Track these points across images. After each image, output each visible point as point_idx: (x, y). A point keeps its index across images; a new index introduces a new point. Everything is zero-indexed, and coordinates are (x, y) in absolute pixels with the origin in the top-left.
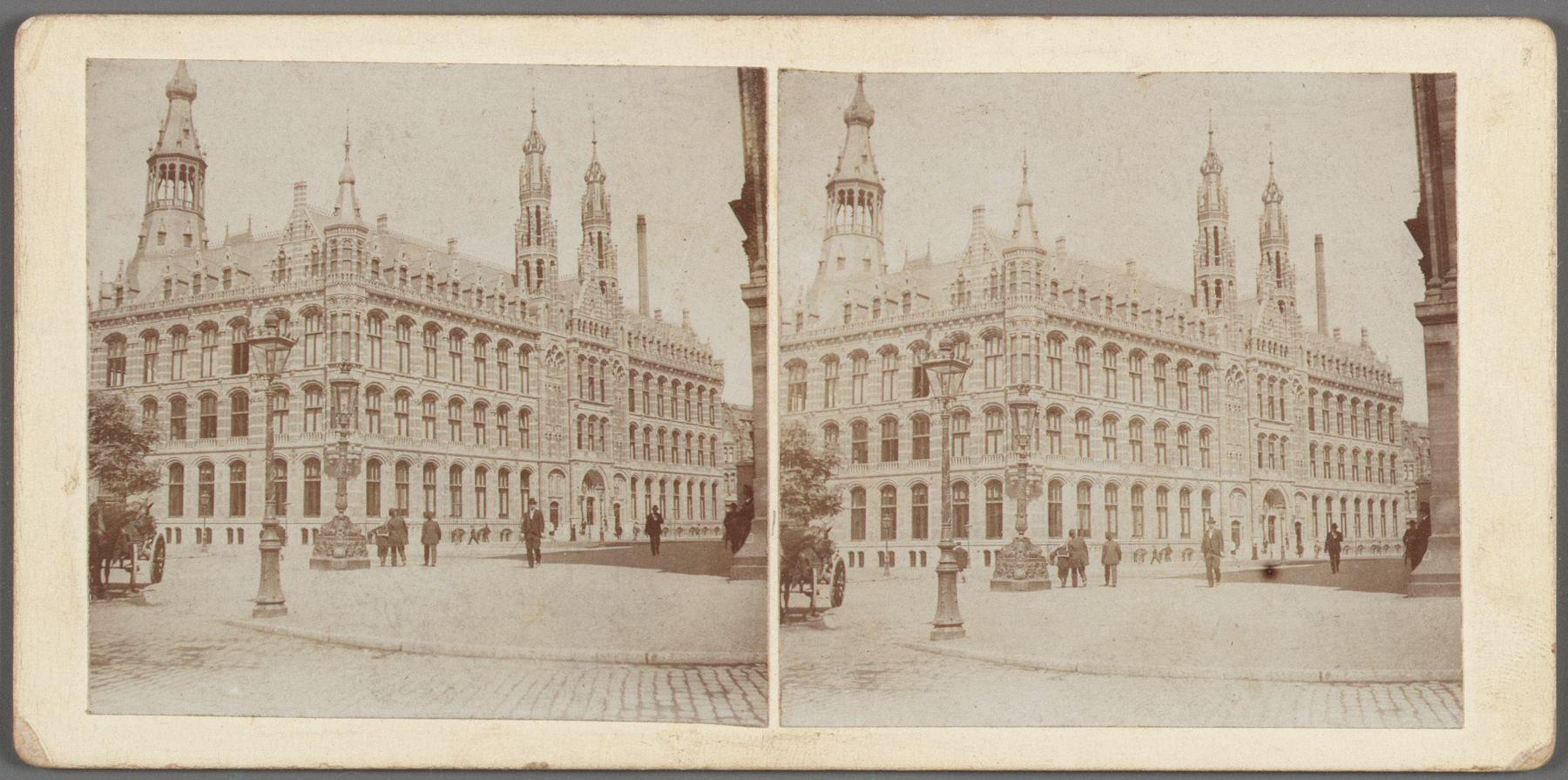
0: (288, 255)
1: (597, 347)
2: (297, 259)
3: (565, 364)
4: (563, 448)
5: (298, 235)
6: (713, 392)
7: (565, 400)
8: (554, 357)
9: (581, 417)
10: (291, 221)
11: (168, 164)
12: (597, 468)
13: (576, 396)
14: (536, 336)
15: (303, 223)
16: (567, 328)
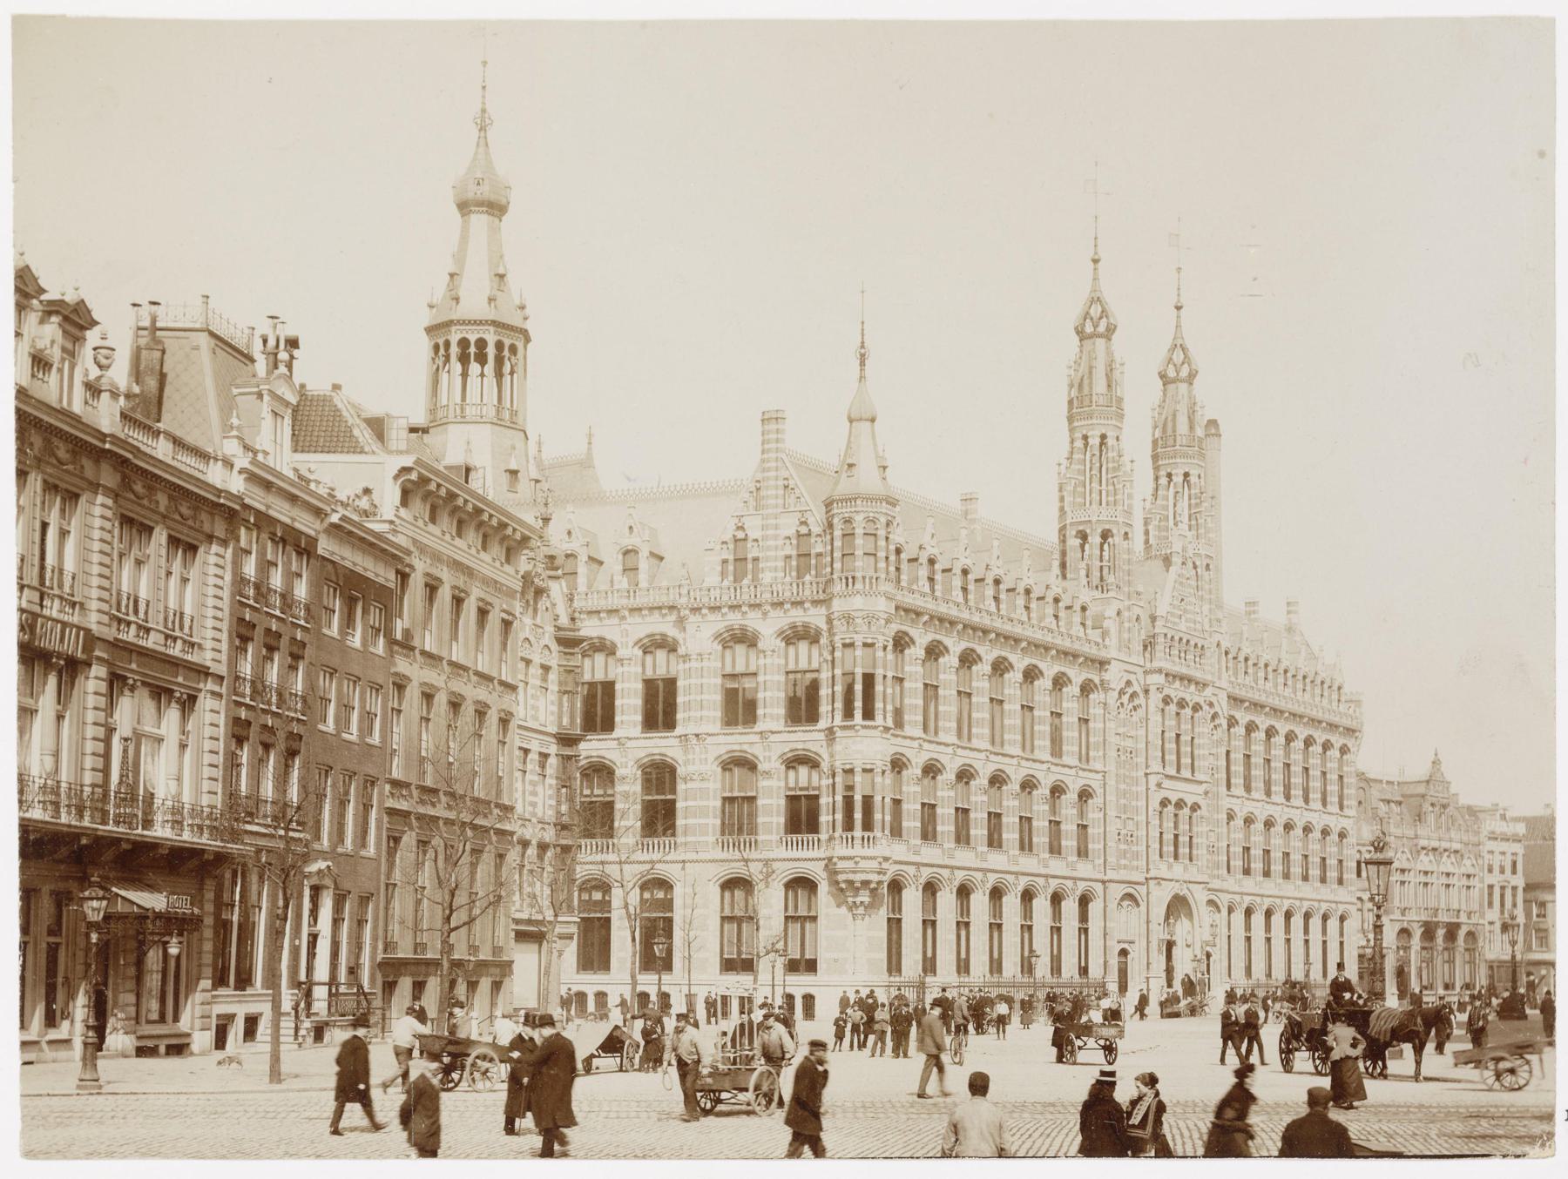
0: (752, 535)
1: (1186, 679)
2: (771, 543)
3: (1141, 712)
4: (1136, 856)
5: (772, 502)
6: (1344, 750)
7: (1141, 773)
8: (1125, 699)
9: (1164, 803)
10: (759, 476)
11: (473, 338)
12: (1184, 892)
13: (1156, 766)
14: (1102, 664)
15: (781, 483)
16: (1145, 647)
